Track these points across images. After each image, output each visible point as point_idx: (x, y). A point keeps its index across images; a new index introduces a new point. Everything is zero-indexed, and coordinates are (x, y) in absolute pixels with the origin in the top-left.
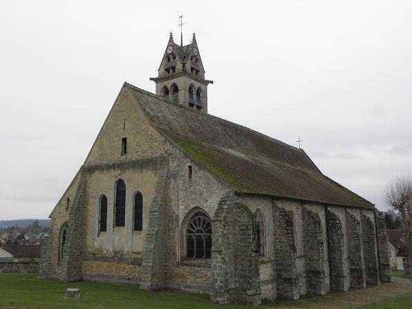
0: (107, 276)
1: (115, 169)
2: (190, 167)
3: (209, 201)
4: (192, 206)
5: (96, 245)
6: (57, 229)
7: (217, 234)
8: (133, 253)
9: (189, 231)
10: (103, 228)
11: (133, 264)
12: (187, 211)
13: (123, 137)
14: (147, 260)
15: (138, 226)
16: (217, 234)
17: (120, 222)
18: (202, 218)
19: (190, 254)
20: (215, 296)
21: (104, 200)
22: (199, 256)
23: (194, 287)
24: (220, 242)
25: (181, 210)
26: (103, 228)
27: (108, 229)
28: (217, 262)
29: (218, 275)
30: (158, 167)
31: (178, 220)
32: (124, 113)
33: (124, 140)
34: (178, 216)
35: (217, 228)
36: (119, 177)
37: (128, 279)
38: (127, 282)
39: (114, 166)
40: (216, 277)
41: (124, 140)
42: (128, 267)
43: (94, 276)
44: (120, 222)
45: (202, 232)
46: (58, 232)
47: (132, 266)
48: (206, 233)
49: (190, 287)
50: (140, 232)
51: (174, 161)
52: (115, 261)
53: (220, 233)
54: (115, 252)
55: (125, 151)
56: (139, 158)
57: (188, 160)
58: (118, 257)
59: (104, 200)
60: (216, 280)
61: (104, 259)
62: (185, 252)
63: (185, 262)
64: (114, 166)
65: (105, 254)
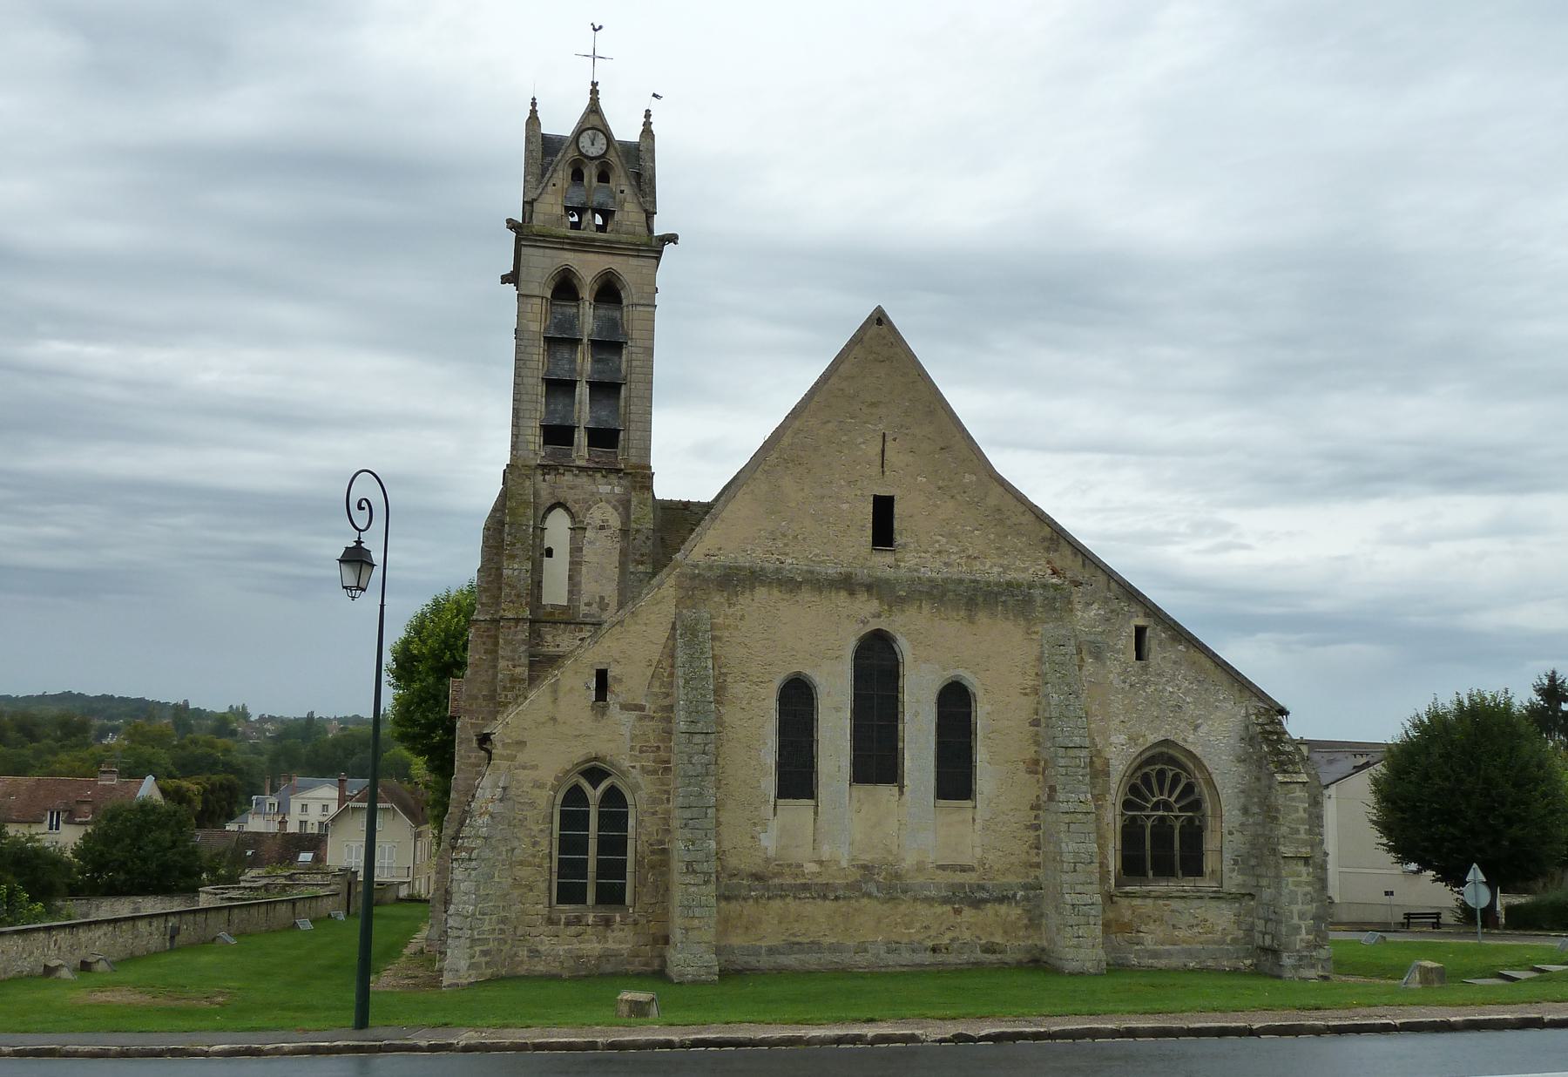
0: (834, 949)
1: (852, 593)
2: (1140, 632)
3: (1203, 730)
5: (769, 842)
6: (539, 785)
7: (1294, 816)
8: (942, 867)
10: (797, 778)
11: (945, 901)
14: (1079, 888)
15: (955, 779)
16: (1294, 816)
17: (877, 761)
20: (1296, 967)
22: (1164, 869)
23: (1169, 954)
24: (1303, 836)
26: (797, 778)
28: (1298, 884)
29: (1302, 916)
30: (1039, 612)
31: (1108, 774)
33: (883, 509)
34: (1107, 763)
35: (1293, 799)
36: (874, 625)
37: (934, 950)
38: (928, 958)
39: (846, 584)
40: (1296, 921)
41: (883, 509)
42: (922, 909)
43: (771, 951)
44: (877, 761)
47: (948, 908)
48: (1181, 809)
49: (1155, 955)
50: (968, 803)
51: (1088, 604)
52: (869, 895)
53: (1302, 814)
54: (865, 867)
55: (883, 533)
56: (954, 573)
58: (880, 883)
61: (823, 892)
62: (1114, 863)
63: (1128, 889)
64: (846, 584)
65: (820, 874)
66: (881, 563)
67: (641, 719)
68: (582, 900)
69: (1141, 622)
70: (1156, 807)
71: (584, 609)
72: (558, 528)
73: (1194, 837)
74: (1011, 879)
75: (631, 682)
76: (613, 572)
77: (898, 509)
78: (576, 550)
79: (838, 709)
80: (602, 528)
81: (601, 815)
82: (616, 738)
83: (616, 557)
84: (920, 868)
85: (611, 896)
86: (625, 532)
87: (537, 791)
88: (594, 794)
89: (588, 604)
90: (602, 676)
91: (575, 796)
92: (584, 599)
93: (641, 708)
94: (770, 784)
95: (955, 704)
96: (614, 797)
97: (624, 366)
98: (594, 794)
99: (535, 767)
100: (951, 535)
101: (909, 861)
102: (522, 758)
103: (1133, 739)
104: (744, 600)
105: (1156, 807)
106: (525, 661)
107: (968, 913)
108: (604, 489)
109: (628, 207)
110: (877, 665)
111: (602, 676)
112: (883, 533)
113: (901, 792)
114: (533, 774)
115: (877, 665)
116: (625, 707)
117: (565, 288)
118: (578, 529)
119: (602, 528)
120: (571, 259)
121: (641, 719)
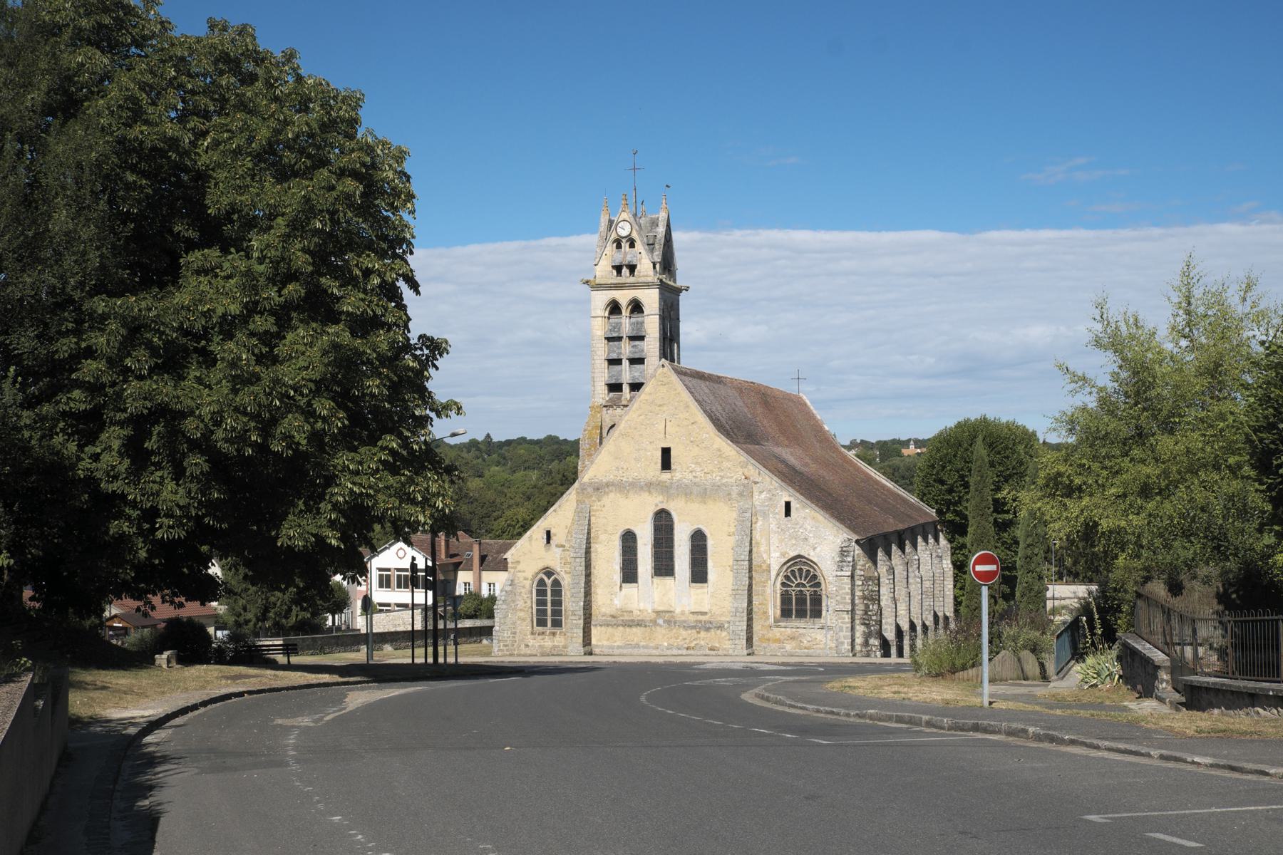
2: (788, 505)
4: (792, 554)
5: (618, 603)
6: (526, 579)
8: (693, 613)
9: (783, 584)
10: (629, 575)
12: (784, 560)
13: (665, 446)
15: (699, 574)
17: (664, 567)
18: (805, 568)
19: (786, 613)
21: (629, 540)
22: (801, 614)
25: (774, 556)
26: (629, 575)
27: (639, 580)
32: (665, 408)
33: (666, 452)
34: (769, 566)
38: (685, 652)
39: (649, 486)
41: (666, 452)
42: (684, 633)
43: (619, 647)
44: (664, 567)
45: (804, 585)
46: (528, 583)
55: (666, 463)
57: (784, 493)
58: (667, 618)
59: (629, 540)
60: (843, 643)
61: (639, 624)
64: (649, 486)
66: (666, 476)
68: (545, 625)
69: (787, 499)
70: (798, 585)
73: (817, 600)
74: (723, 619)
77: (672, 453)
82: (553, 558)
84: (683, 613)
85: (557, 624)
88: (549, 582)
90: (548, 533)
94: (618, 576)
96: (557, 583)
98: (549, 582)
100: (697, 463)
101: (678, 611)
102: (519, 567)
103: (783, 555)
105: (798, 585)
107: (703, 634)
109: (643, 261)
110: (663, 524)
111: (548, 533)
112: (666, 463)
115: (663, 524)
116: (557, 546)
117: (614, 308)
120: (632, 280)
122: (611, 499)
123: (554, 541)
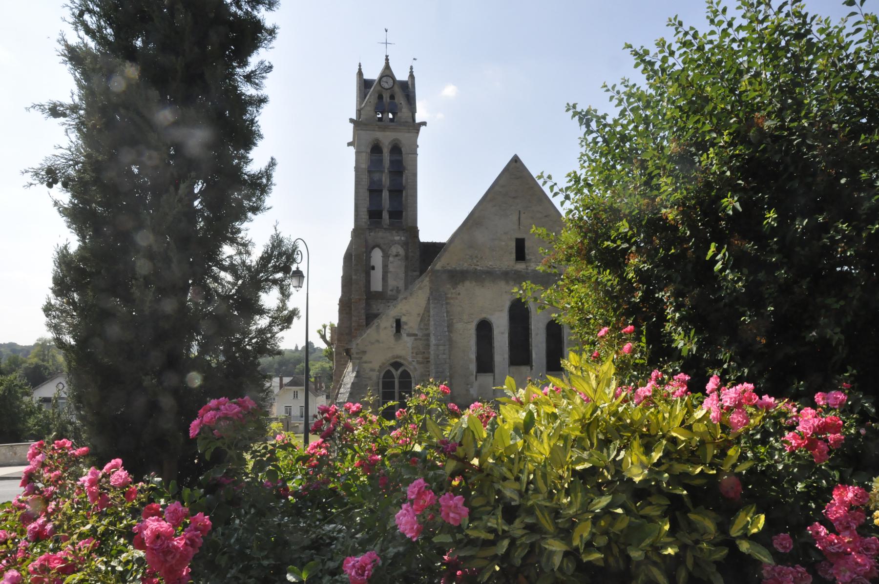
6: (372, 370)
13: (520, 236)
21: (484, 329)
33: (520, 245)
41: (520, 245)
59: (484, 329)
67: (416, 340)
71: (389, 293)
72: (377, 257)
75: (411, 323)
76: (402, 275)
77: (527, 244)
78: (385, 266)
79: (503, 333)
80: (396, 256)
81: (400, 382)
83: (403, 269)
86: (407, 258)
87: (371, 373)
88: (396, 374)
89: (392, 290)
91: (388, 375)
92: (390, 288)
93: (416, 335)
94: (473, 367)
95: (554, 331)
97: (404, 181)
98: (396, 374)
99: (370, 362)
102: (365, 358)
104: (461, 288)
106: (364, 317)
108: (397, 238)
110: (519, 314)
112: (521, 253)
113: (531, 369)
114: (370, 365)
116: (409, 335)
117: (376, 149)
118: (386, 256)
119: (396, 256)
120: (379, 135)
121: (416, 340)
122: (467, 288)
123: (405, 329)
